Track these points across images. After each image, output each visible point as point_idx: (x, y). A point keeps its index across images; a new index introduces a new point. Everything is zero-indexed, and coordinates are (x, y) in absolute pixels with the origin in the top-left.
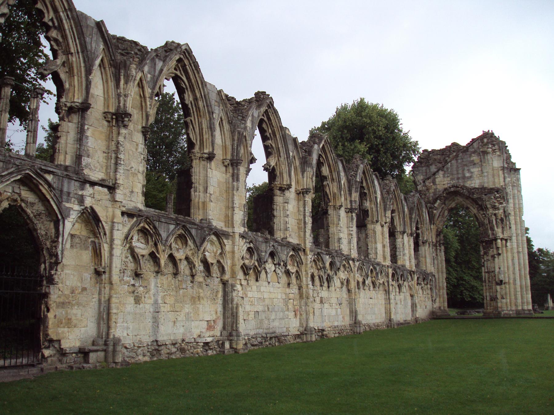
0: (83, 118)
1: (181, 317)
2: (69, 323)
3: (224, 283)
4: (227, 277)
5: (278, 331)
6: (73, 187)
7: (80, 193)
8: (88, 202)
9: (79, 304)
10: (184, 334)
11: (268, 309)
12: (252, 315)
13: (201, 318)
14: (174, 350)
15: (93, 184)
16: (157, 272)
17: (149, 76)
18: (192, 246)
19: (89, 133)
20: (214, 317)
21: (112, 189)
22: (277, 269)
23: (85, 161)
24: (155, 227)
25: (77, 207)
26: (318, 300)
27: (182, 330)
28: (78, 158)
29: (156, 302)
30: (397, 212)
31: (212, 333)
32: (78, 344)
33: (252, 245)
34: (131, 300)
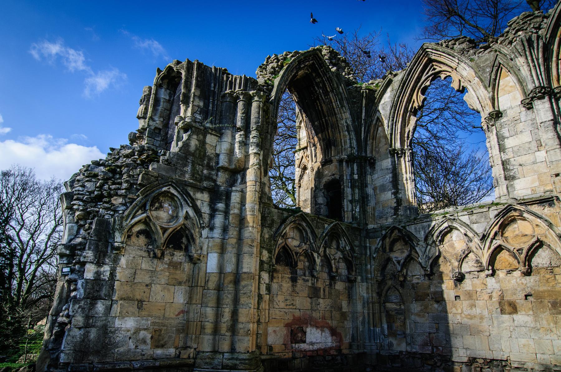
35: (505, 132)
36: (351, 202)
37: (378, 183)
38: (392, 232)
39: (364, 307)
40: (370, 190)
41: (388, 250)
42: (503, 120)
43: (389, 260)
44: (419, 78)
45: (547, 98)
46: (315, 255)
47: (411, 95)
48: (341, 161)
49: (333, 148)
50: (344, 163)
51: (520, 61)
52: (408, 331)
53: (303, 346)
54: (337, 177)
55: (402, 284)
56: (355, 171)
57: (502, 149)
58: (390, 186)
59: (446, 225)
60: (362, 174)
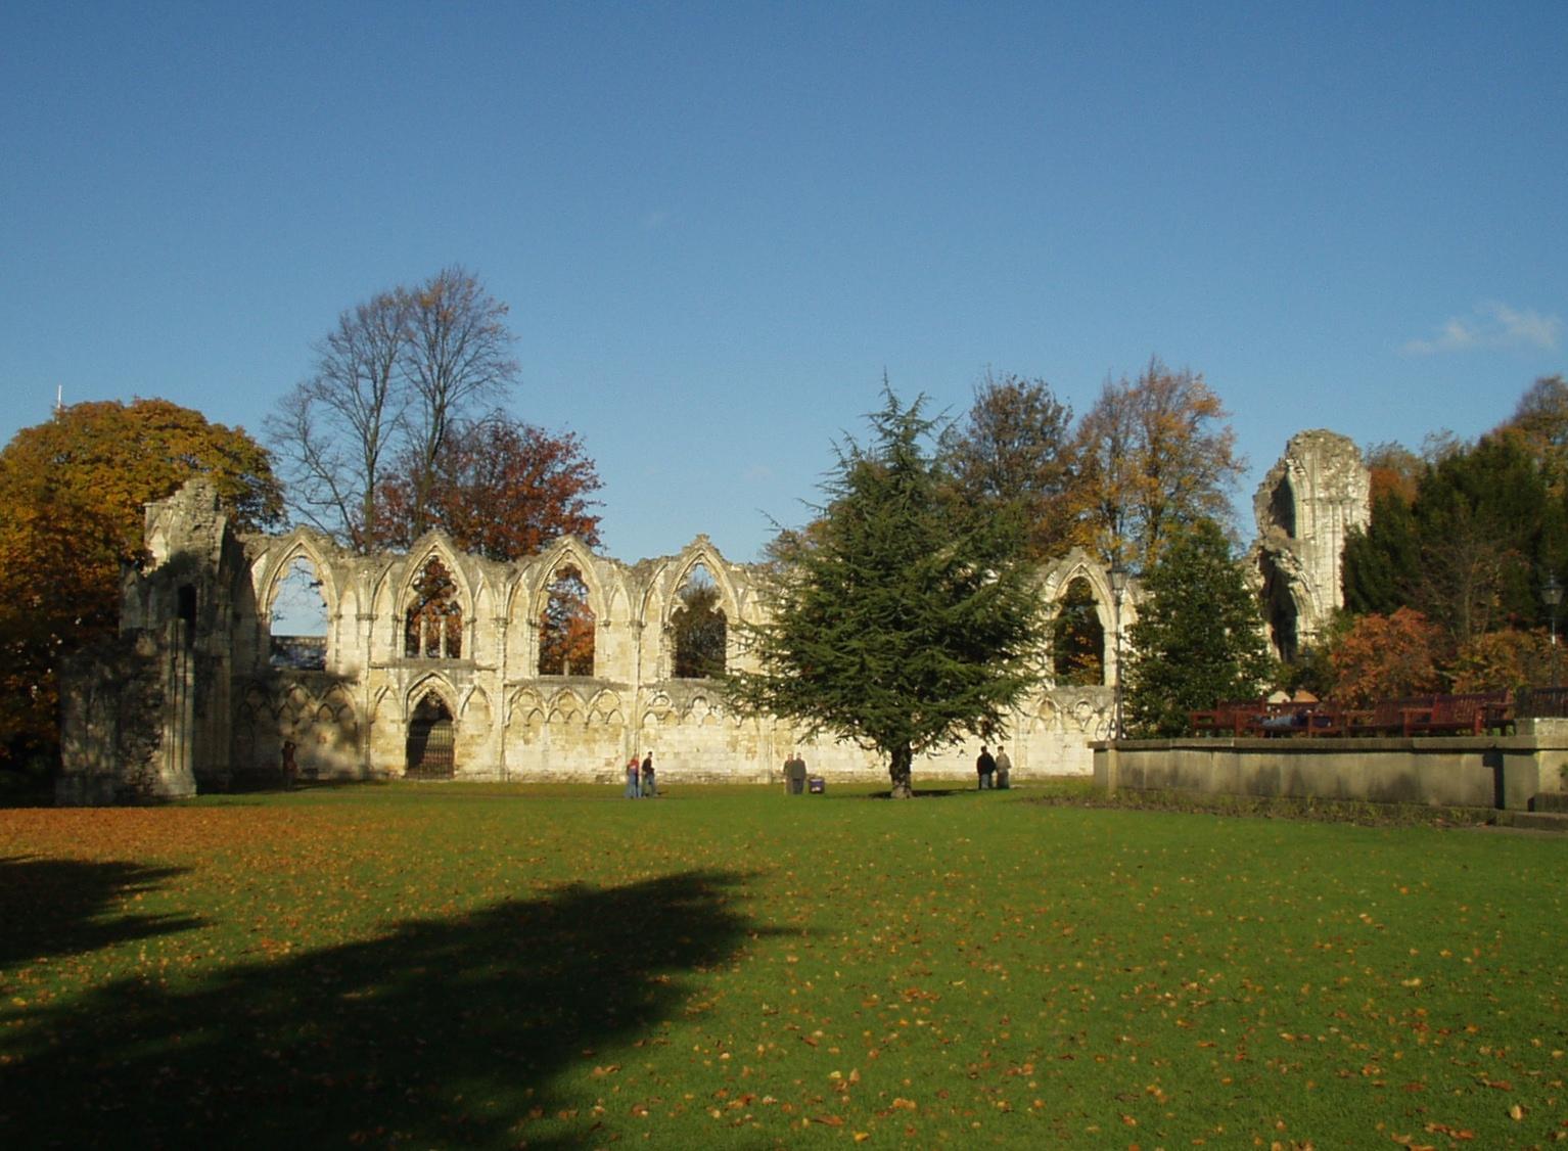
0: (474, 627)
2: (469, 755)
3: (625, 727)
4: (626, 722)
5: (714, 771)
8: (476, 682)
9: (477, 744)
15: (479, 669)
18: (581, 701)
19: (478, 636)
20: (614, 756)
21: (494, 670)
23: (476, 655)
25: (469, 686)
28: (472, 653)
30: (1101, 602)
31: (610, 768)
32: (476, 769)
33: (664, 693)
34: (522, 742)
35: (341, 630)
51: (362, 590)
55: (254, 722)
57: (338, 641)
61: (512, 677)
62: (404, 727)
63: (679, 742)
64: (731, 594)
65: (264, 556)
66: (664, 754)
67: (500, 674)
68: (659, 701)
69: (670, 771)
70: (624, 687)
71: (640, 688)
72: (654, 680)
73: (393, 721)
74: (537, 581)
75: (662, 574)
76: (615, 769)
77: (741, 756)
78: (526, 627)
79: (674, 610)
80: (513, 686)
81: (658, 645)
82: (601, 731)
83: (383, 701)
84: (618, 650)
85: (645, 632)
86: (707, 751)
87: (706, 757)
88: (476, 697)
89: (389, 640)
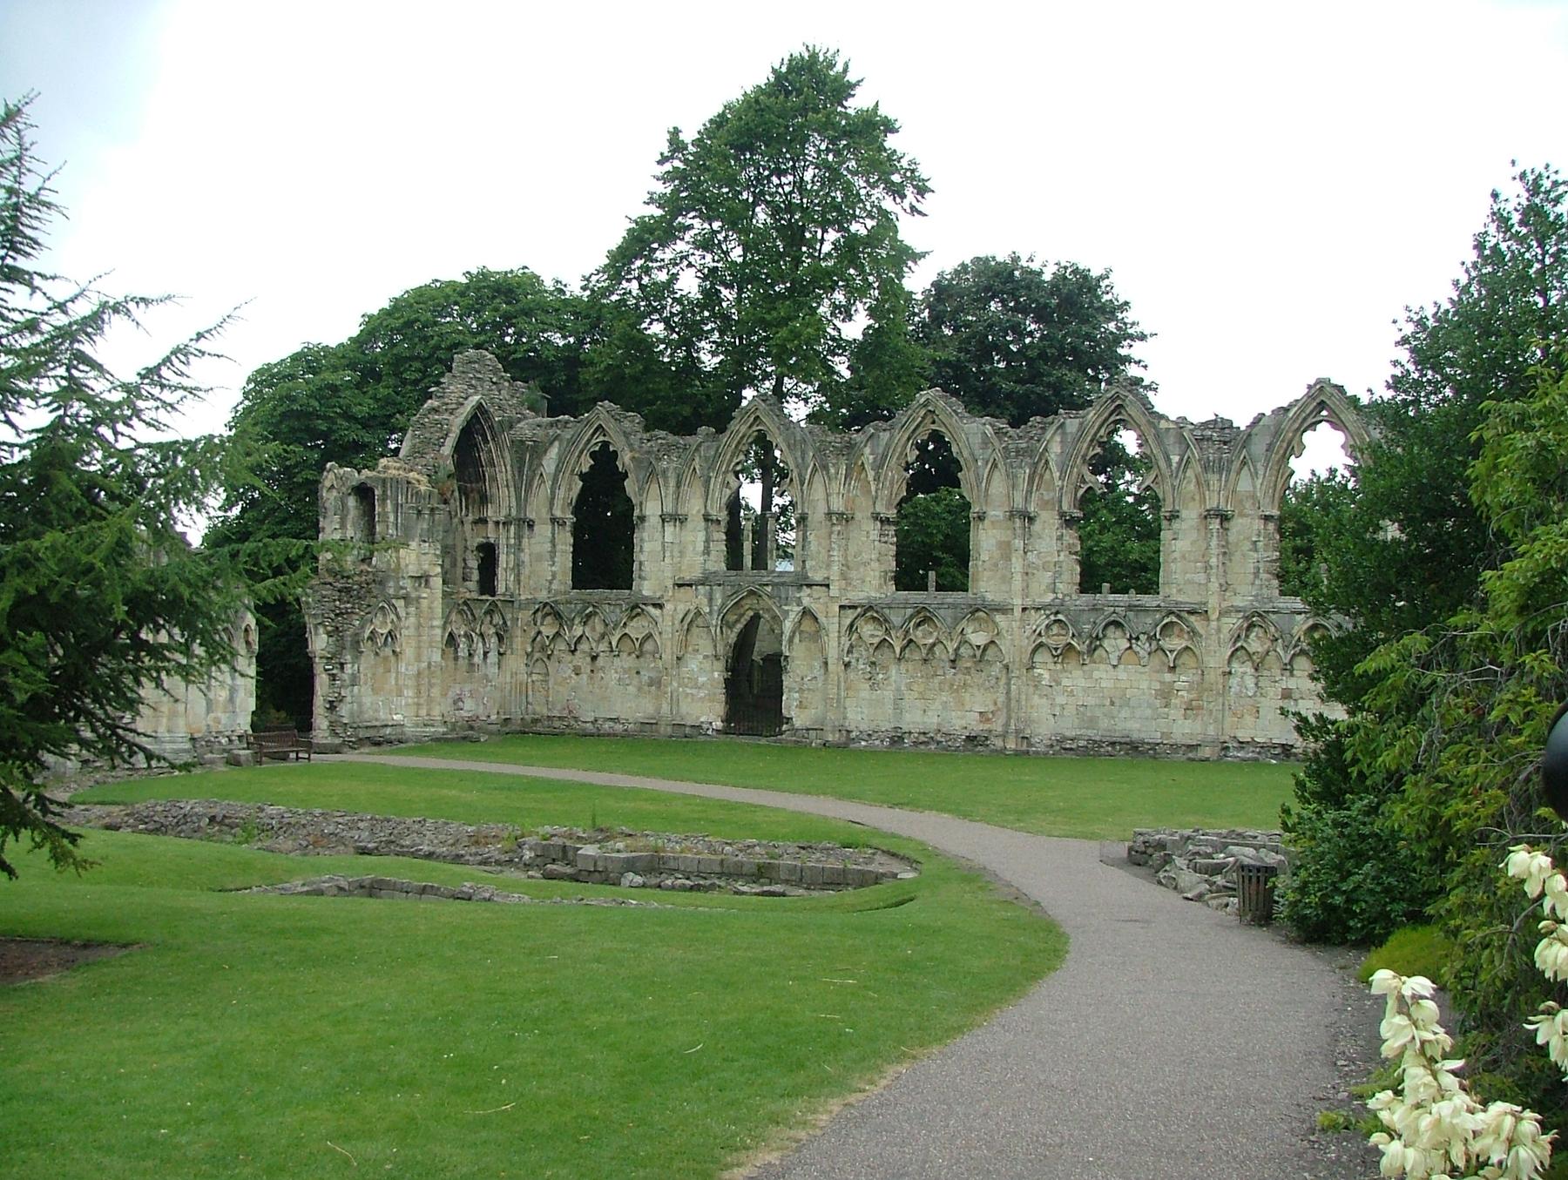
1: (937, 705)
5: (1135, 736)
6: (792, 592)
7: (798, 595)
8: (806, 601)
10: (939, 724)
11: (1112, 703)
12: (1070, 710)
13: (967, 708)
14: (922, 739)
15: (809, 586)
16: (899, 659)
17: (871, 457)
20: (992, 708)
22: (1134, 646)
24: (882, 615)
26: (1273, 692)
27: (935, 720)
29: (898, 689)
33: (1060, 617)
36: (506, 570)
37: (537, 549)
38: (544, 607)
39: (512, 677)
40: (525, 557)
41: (538, 623)
42: (646, 524)
43: (539, 633)
44: (589, 441)
45: (672, 523)
46: (473, 634)
47: (579, 457)
48: (497, 523)
49: (489, 505)
50: (501, 526)
52: (550, 699)
53: (462, 713)
54: (492, 541)
55: (549, 657)
56: (512, 535)
58: (548, 556)
59: (590, 609)
60: (519, 537)
61: (857, 596)
62: (720, 665)
63: (1085, 690)
64: (1162, 464)
65: (556, 444)
66: (1063, 707)
67: (834, 591)
68: (1055, 629)
69: (1068, 734)
70: (1004, 610)
71: (1024, 609)
72: (1049, 598)
73: (706, 657)
74: (884, 457)
75: (1058, 438)
76: (993, 727)
77: (1176, 713)
78: (873, 529)
79: (1081, 492)
80: (855, 607)
81: (1055, 546)
82: (973, 671)
83: (695, 630)
84: (997, 554)
85: (1037, 527)
86: (1126, 703)
87: (1125, 713)
88: (808, 625)
89: (700, 547)
